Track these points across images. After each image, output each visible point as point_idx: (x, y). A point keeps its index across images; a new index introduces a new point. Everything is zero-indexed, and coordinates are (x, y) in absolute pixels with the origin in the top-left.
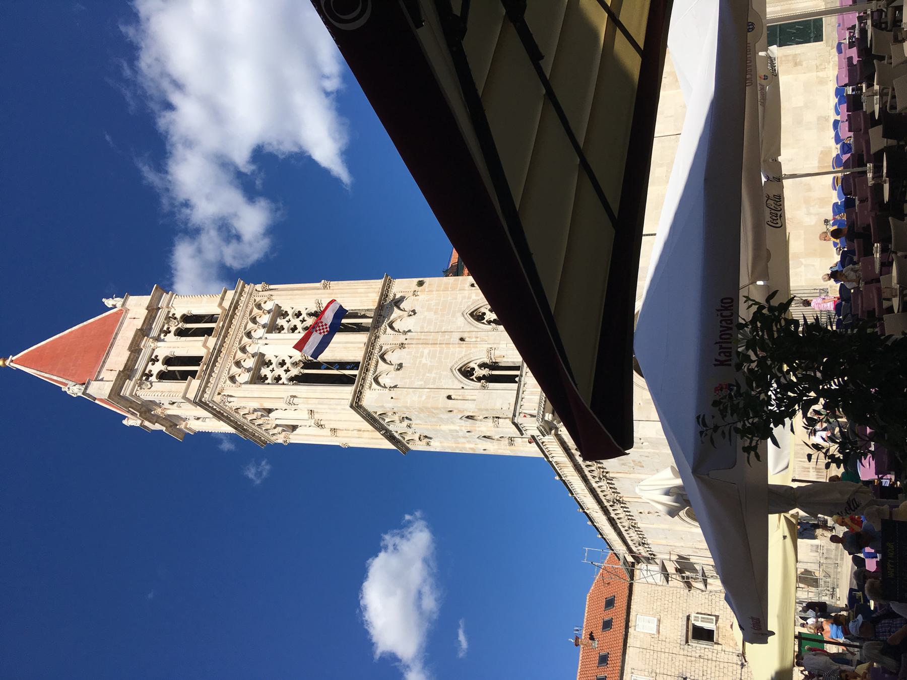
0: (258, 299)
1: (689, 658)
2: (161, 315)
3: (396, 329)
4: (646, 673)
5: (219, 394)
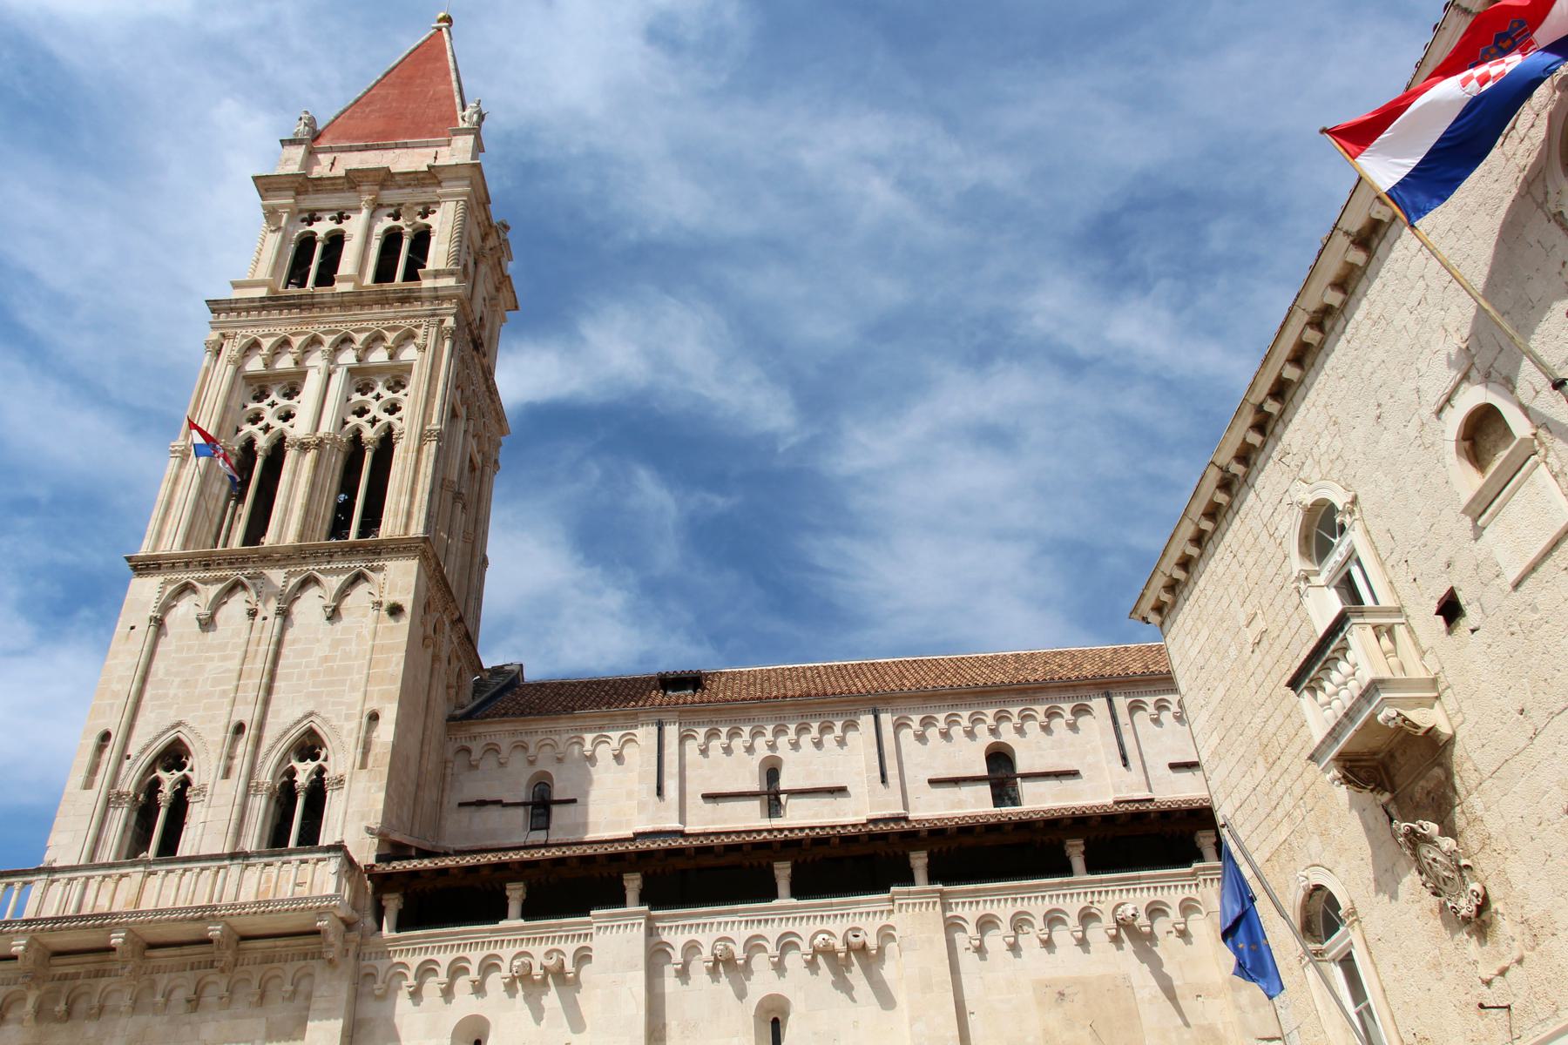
0: (420, 332)
5: (223, 335)
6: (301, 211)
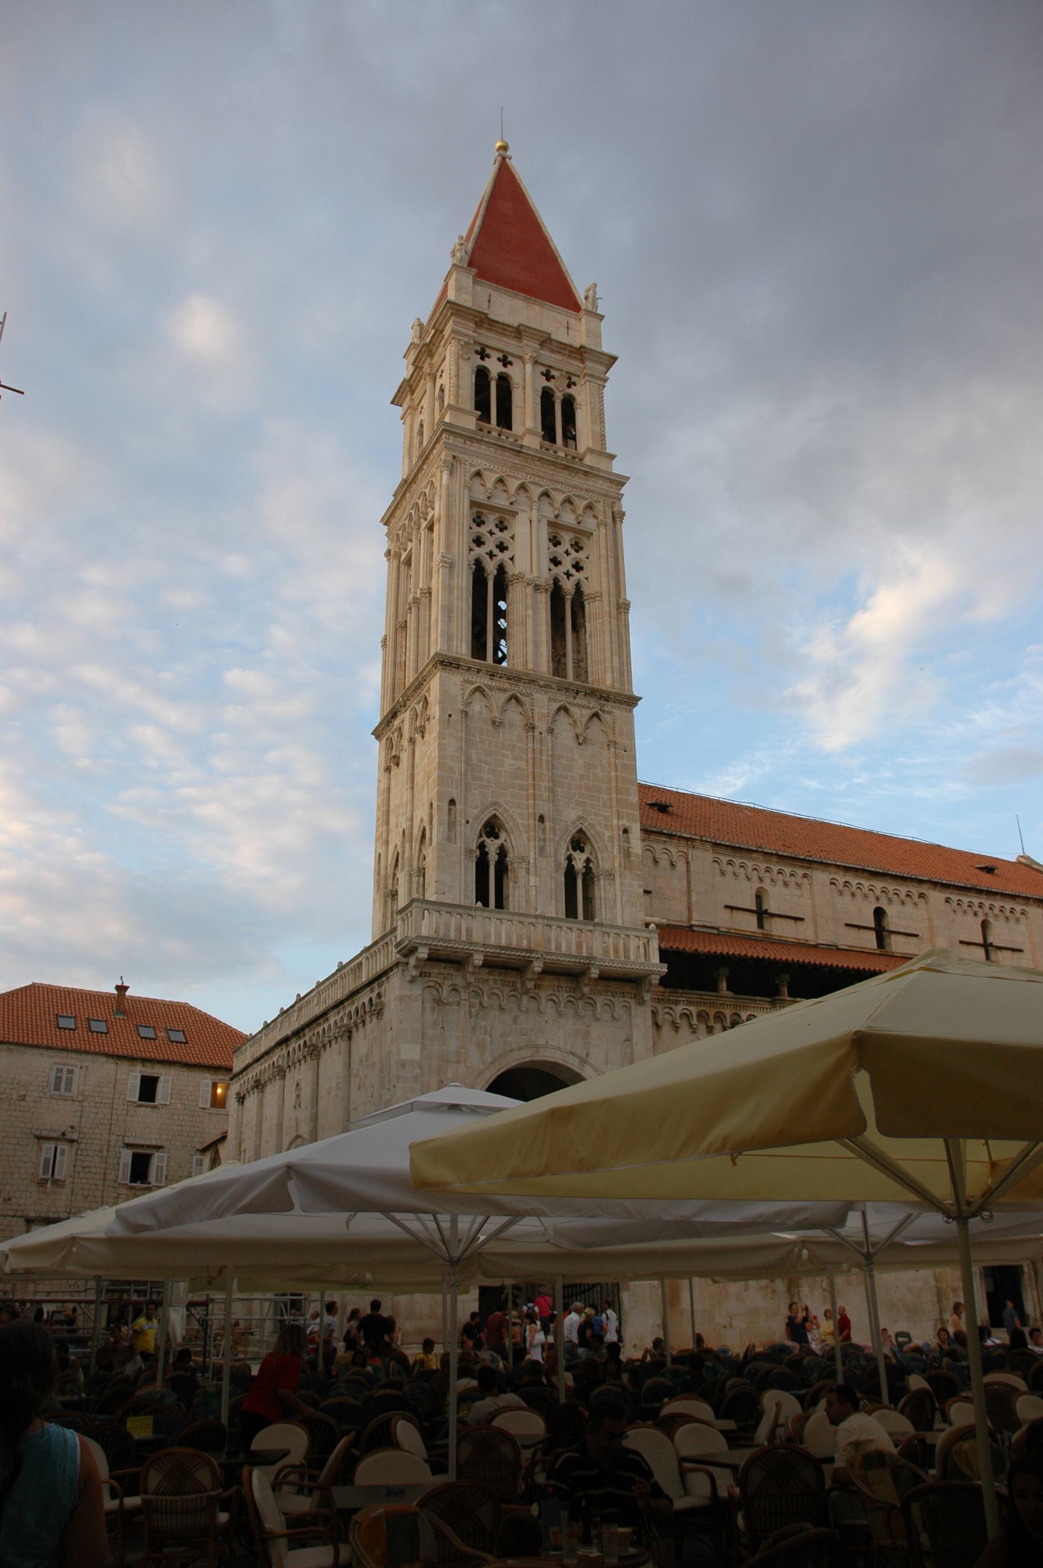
1: (105, 1148)
2: (573, 365)
3: (557, 718)
4: (81, 1088)
5: (454, 457)
6: (476, 342)
